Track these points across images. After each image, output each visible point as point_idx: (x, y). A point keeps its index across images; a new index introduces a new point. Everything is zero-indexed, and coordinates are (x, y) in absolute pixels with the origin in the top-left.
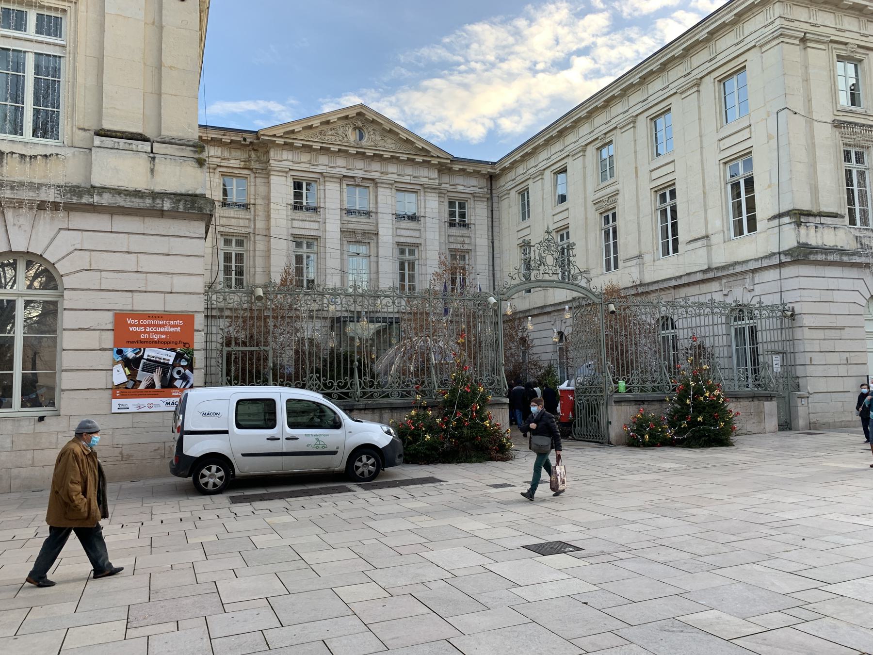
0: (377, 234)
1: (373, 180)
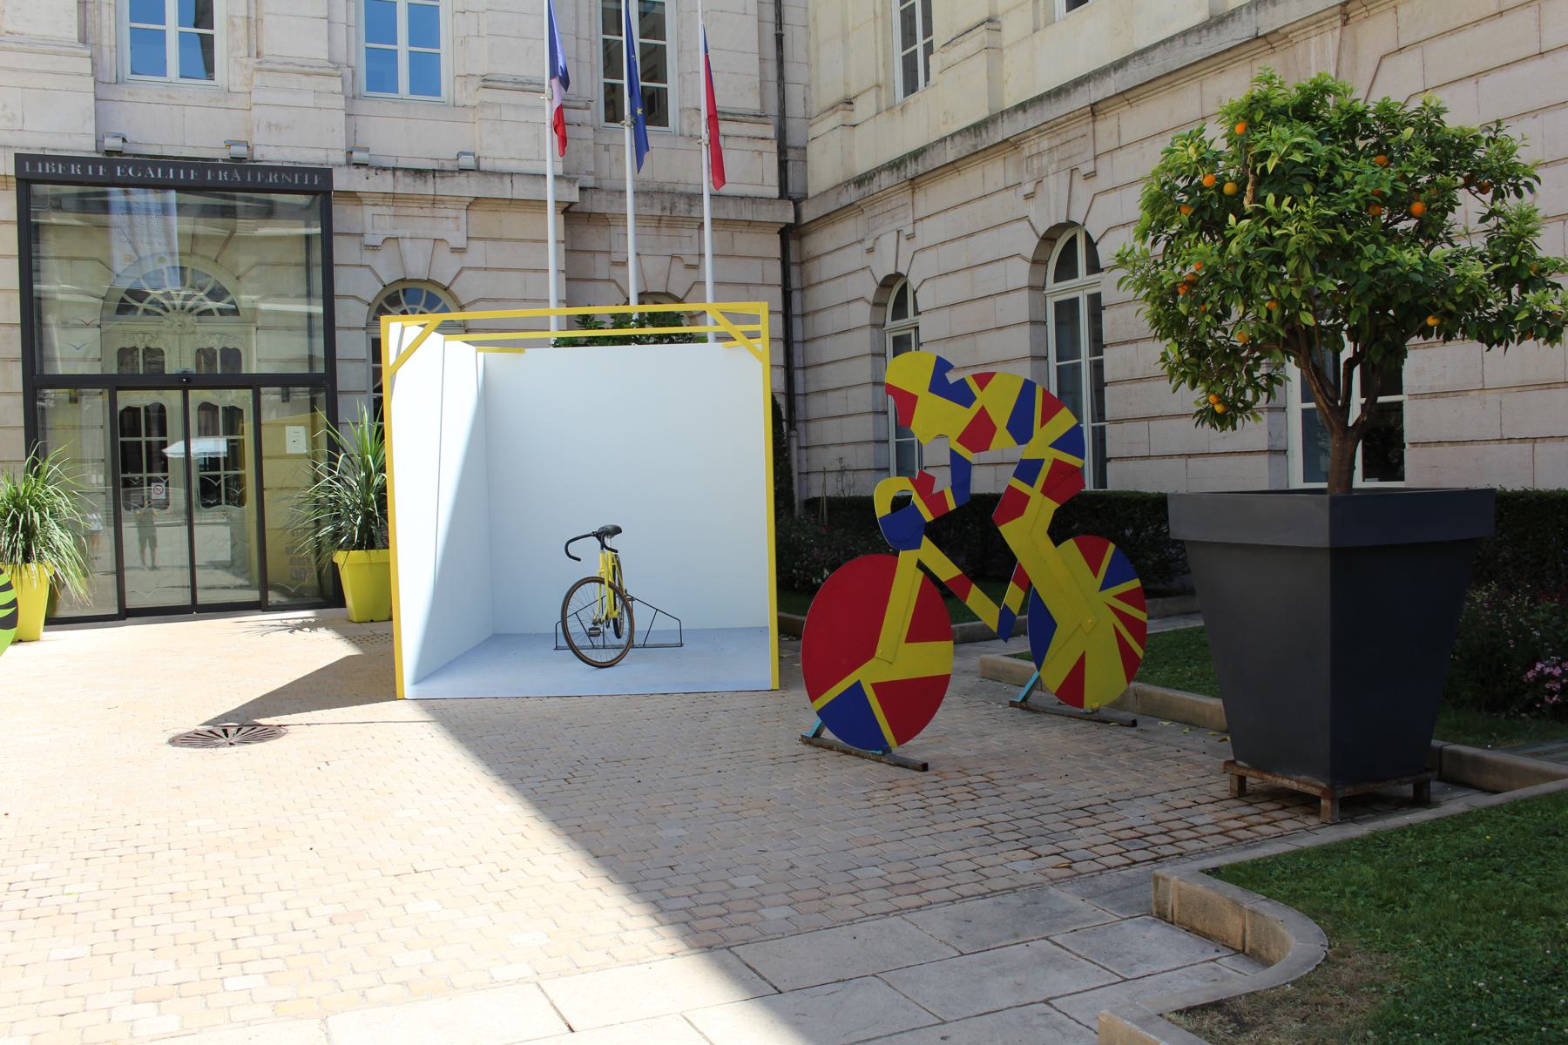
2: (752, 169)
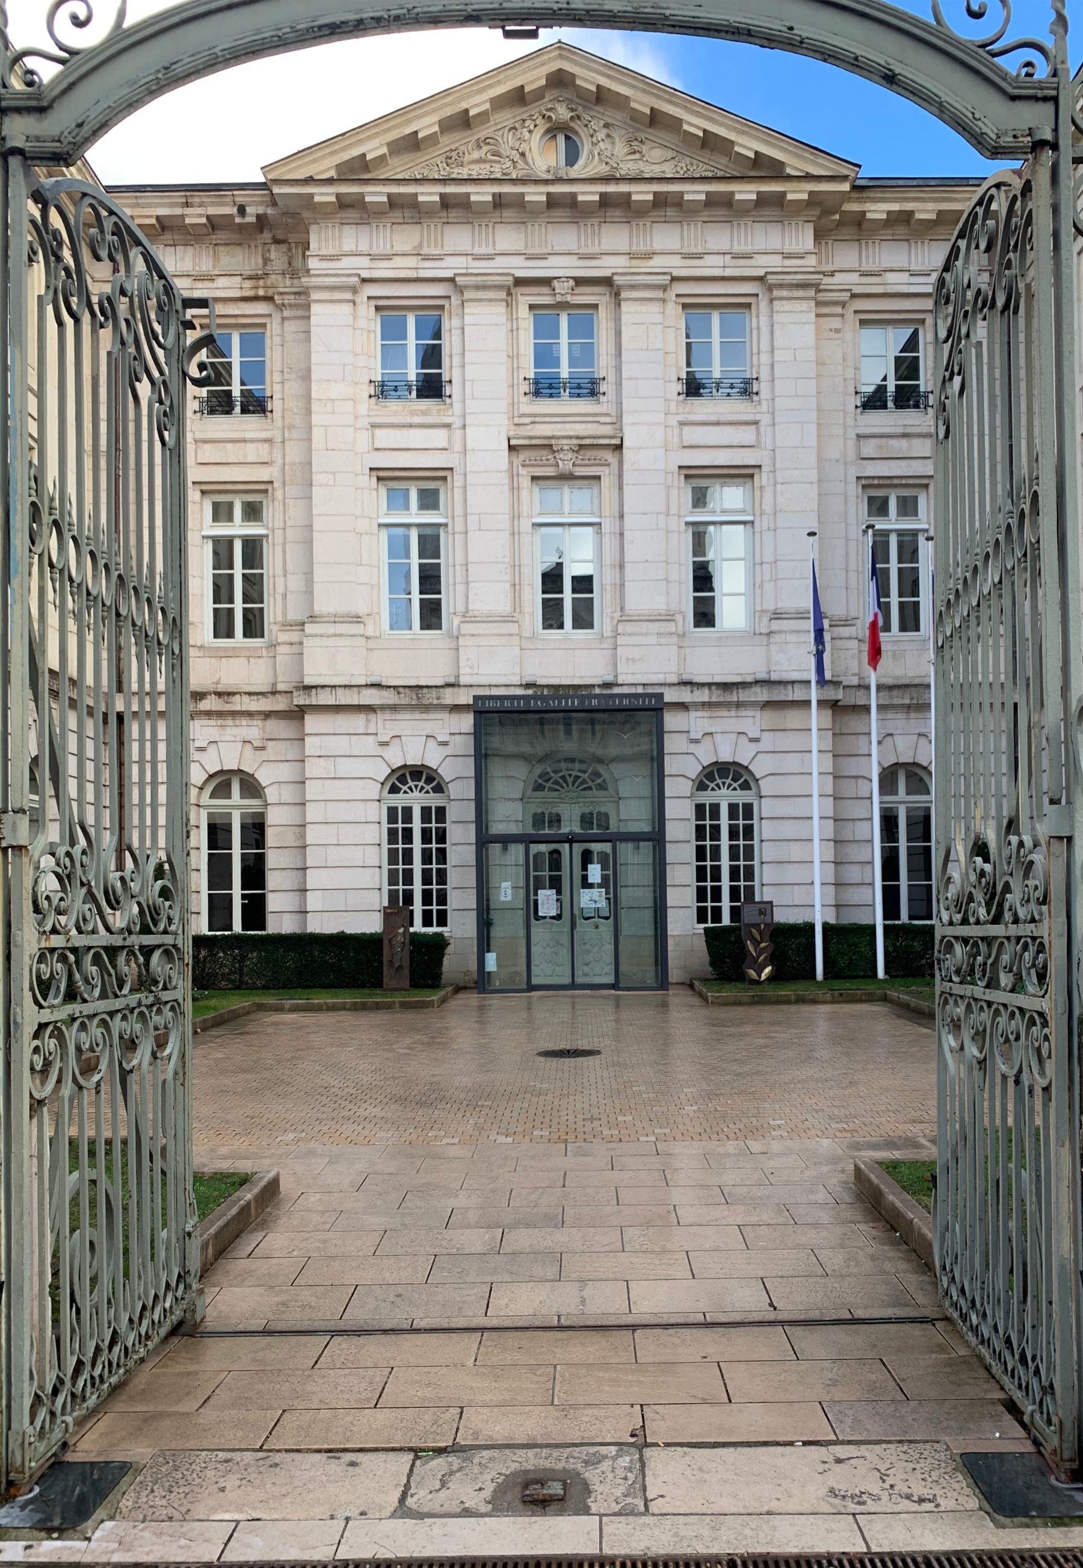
0: (619, 447)
1: (606, 282)
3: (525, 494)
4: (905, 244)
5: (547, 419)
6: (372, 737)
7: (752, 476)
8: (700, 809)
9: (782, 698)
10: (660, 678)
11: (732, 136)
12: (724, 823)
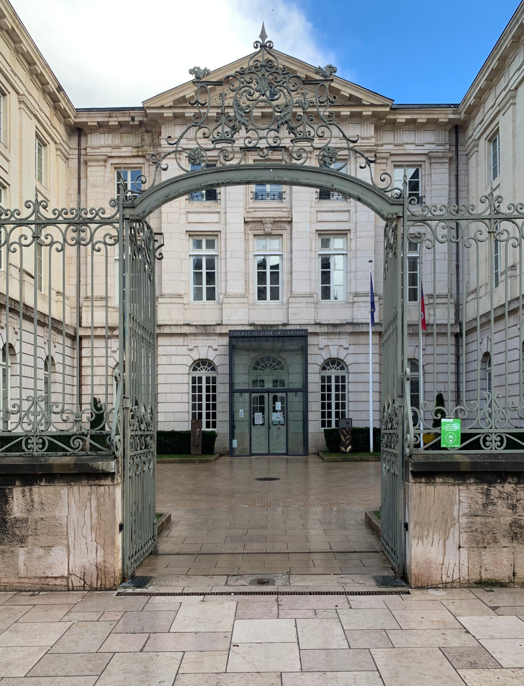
0: (290, 222)
2: (442, 315)
3: (251, 242)
4: (413, 133)
5: (261, 210)
6: (186, 347)
7: (347, 234)
8: (323, 379)
9: (358, 330)
10: (307, 322)
11: (340, 87)
12: (333, 384)
